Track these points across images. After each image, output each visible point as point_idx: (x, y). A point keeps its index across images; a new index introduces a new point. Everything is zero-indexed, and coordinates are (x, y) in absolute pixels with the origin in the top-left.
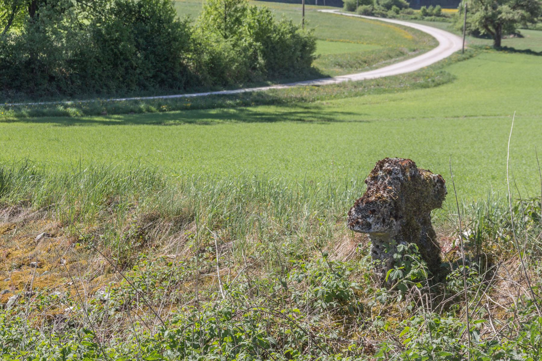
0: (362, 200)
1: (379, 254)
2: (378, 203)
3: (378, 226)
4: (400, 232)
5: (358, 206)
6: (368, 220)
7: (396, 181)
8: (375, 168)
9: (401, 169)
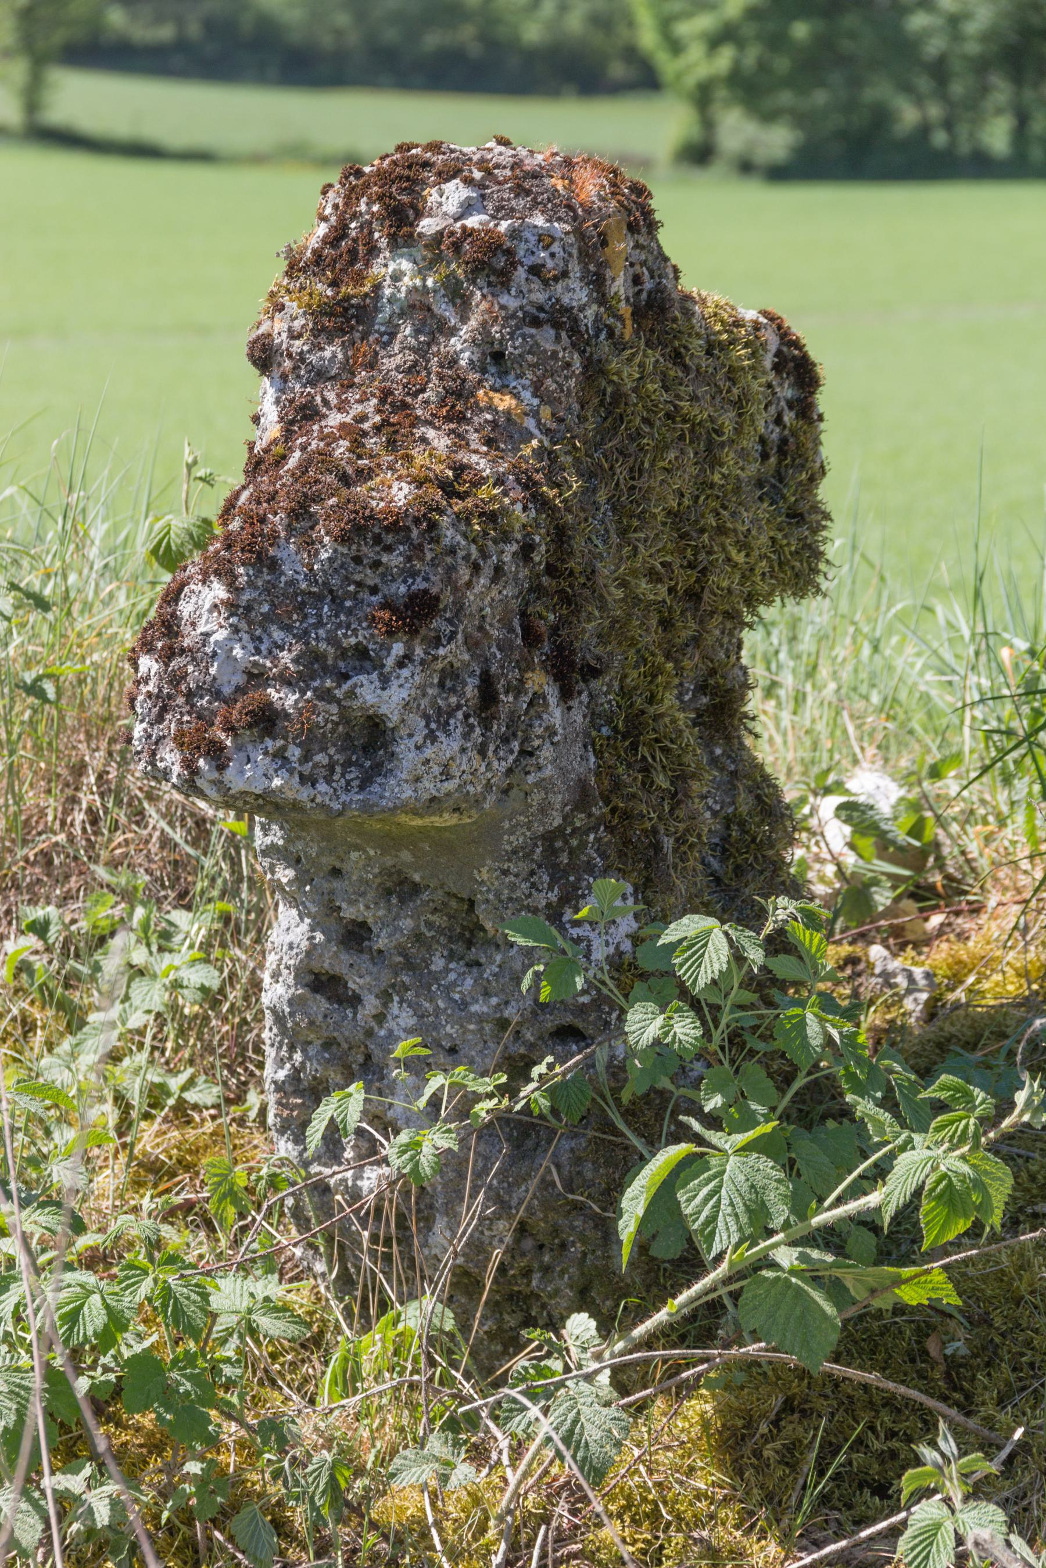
0: (300, 514)
1: (371, 1004)
2: (450, 535)
3: (449, 746)
4: (582, 798)
5: (265, 562)
6: (368, 692)
7: (546, 338)
8: (338, 234)
9: (579, 233)
